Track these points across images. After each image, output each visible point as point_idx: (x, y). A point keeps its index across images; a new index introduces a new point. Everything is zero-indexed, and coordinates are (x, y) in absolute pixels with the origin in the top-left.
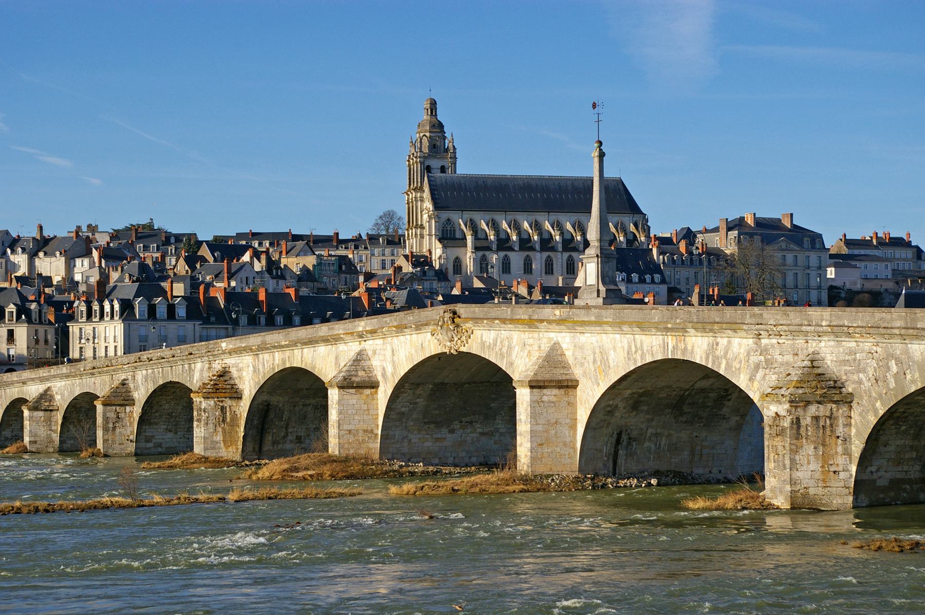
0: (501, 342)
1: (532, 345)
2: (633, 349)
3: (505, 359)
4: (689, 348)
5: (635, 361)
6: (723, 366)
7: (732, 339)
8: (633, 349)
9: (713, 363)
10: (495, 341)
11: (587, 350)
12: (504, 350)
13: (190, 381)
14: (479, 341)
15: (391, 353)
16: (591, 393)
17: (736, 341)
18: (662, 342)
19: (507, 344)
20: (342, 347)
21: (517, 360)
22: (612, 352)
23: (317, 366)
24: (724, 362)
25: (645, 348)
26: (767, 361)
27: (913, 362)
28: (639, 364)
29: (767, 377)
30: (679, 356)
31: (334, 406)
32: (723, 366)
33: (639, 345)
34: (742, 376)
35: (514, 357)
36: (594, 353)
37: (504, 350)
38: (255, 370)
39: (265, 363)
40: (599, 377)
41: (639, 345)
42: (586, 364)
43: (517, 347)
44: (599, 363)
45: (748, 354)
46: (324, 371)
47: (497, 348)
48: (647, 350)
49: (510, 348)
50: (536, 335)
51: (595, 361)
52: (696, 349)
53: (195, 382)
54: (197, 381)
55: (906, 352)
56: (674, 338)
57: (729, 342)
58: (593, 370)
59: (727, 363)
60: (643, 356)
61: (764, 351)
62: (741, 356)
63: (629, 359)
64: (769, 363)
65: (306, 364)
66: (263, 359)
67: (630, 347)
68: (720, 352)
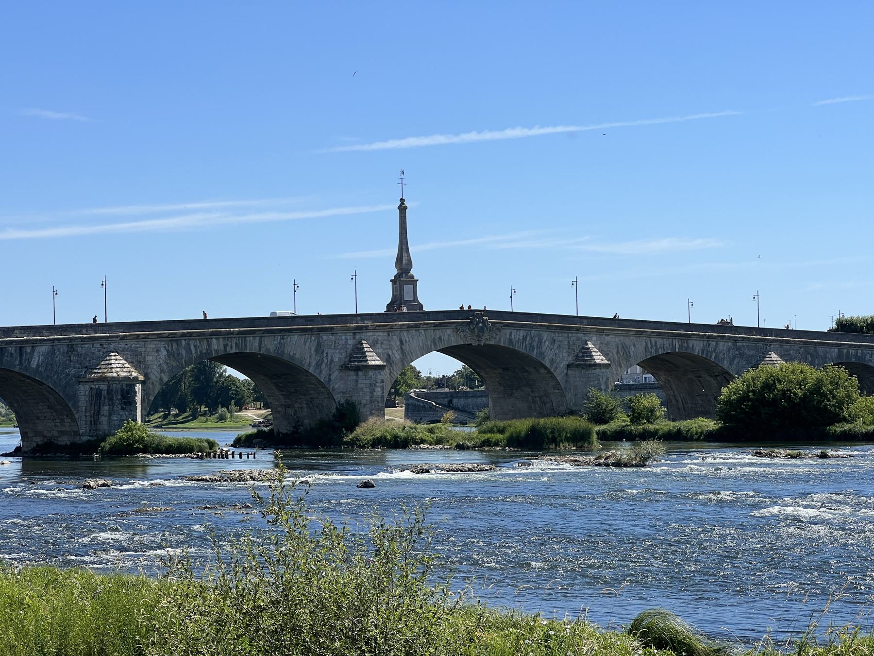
0: (531, 338)
1: (561, 341)
2: (649, 346)
3: (535, 350)
4: (691, 346)
5: (651, 352)
6: (713, 357)
7: (719, 343)
8: (649, 346)
9: (707, 354)
10: (525, 338)
11: (612, 346)
12: (535, 344)
13: (21, 363)
14: (508, 337)
15: (398, 343)
16: (615, 372)
17: (721, 344)
18: (671, 342)
19: (537, 339)
20: (325, 337)
21: (547, 351)
22: (632, 347)
23: (286, 352)
24: (714, 354)
25: (658, 346)
26: (740, 354)
27: (819, 355)
28: (654, 354)
29: (741, 363)
30: (684, 350)
31: (377, 384)
32: (713, 357)
33: (653, 344)
34: (725, 362)
35: (544, 349)
36: (618, 348)
37: (535, 344)
38: (170, 354)
39: (192, 348)
40: (622, 362)
41: (653, 344)
42: (611, 354)
43: (547, 342)
44: (622, 354)
45: (729, 351)
46: (298, 356)
47: (527, 342)
48: (660, 347)
49: (540, 342)
50: (566, 335)
51: (618, 352)
52: (695, 347)
53: (34, 364)
54: (38, 365)
55: (816, 351)
56: (680, 340)
57: (717, 344)
58: (616, 358)
59: (716, 355)
60: (656, 351)
61: (738, 349)
62: (725, 351)
63: (646, 351)
64: (741, 355)
65: (268, 350)
66: (189, 344)
67: (646, 344)
68: (711, 349)
